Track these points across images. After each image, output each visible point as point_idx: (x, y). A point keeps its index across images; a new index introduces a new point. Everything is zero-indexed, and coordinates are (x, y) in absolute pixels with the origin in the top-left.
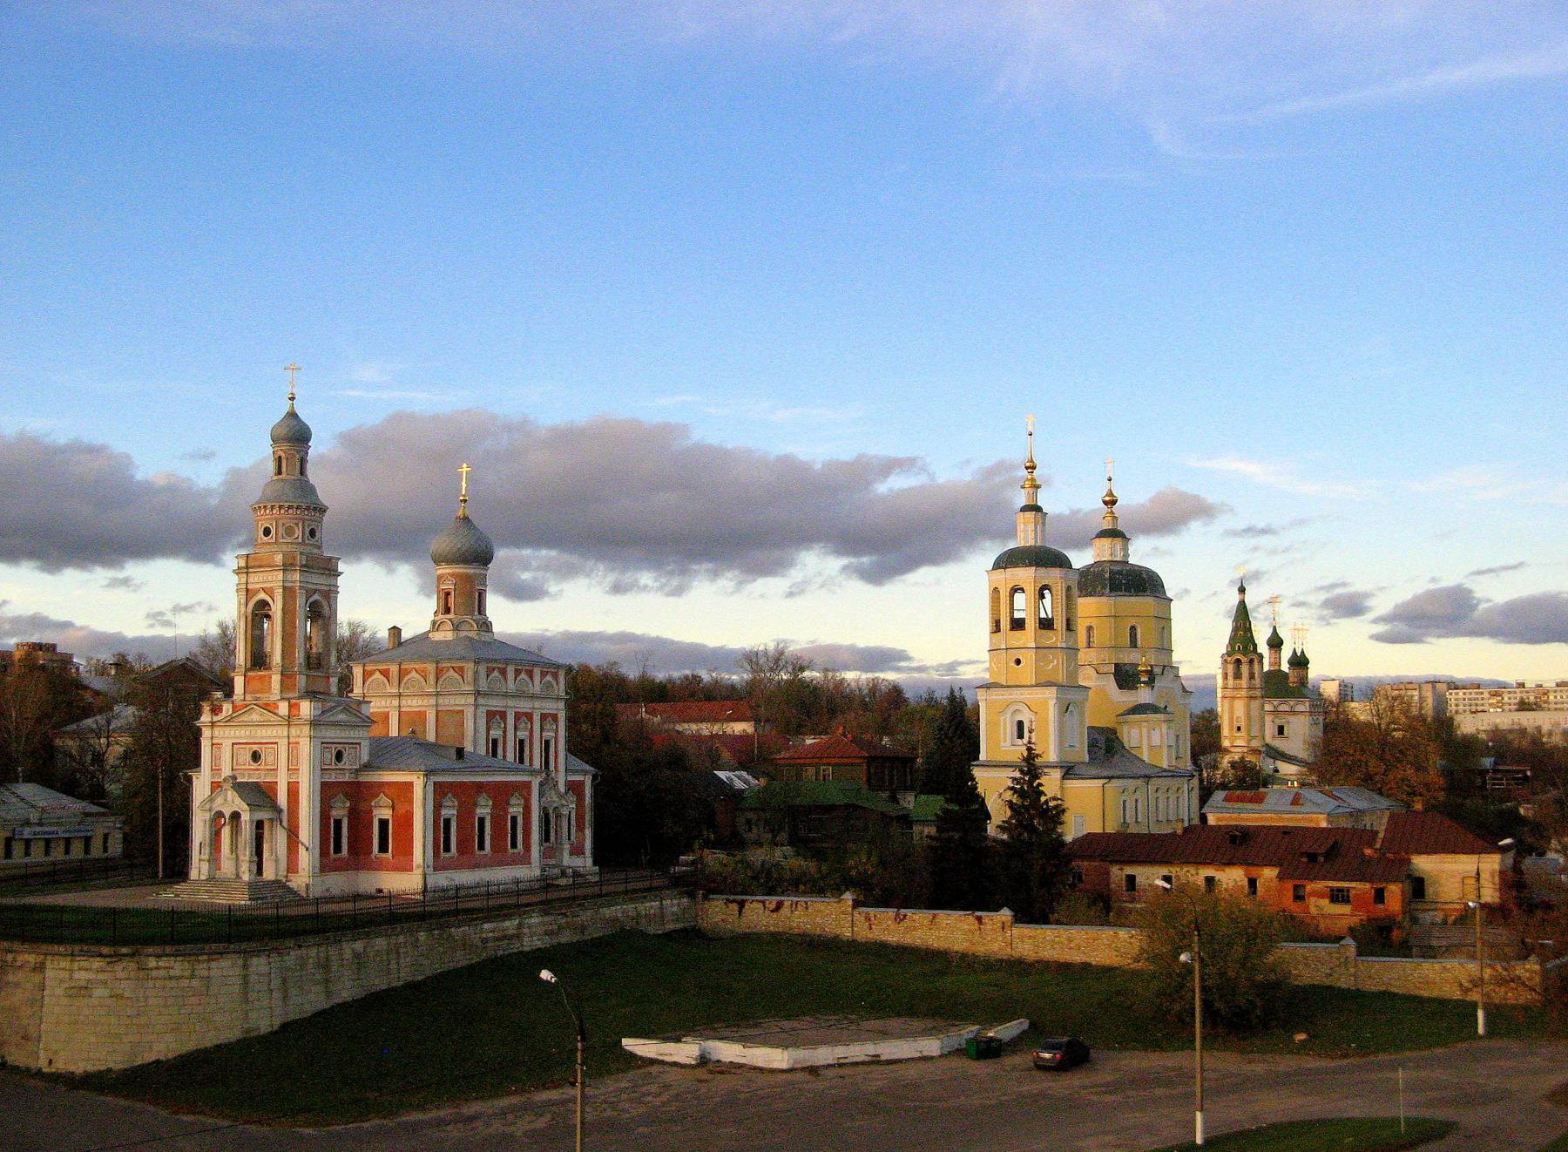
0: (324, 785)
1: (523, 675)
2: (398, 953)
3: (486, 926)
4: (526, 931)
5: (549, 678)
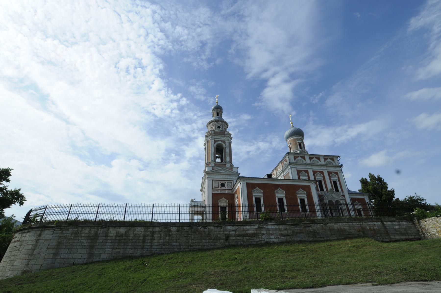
0: (213, 194)
1: (314, 159)
2: (153, 236)
3: (229, 227)
4: (264, 232)
5: (329, 160)
